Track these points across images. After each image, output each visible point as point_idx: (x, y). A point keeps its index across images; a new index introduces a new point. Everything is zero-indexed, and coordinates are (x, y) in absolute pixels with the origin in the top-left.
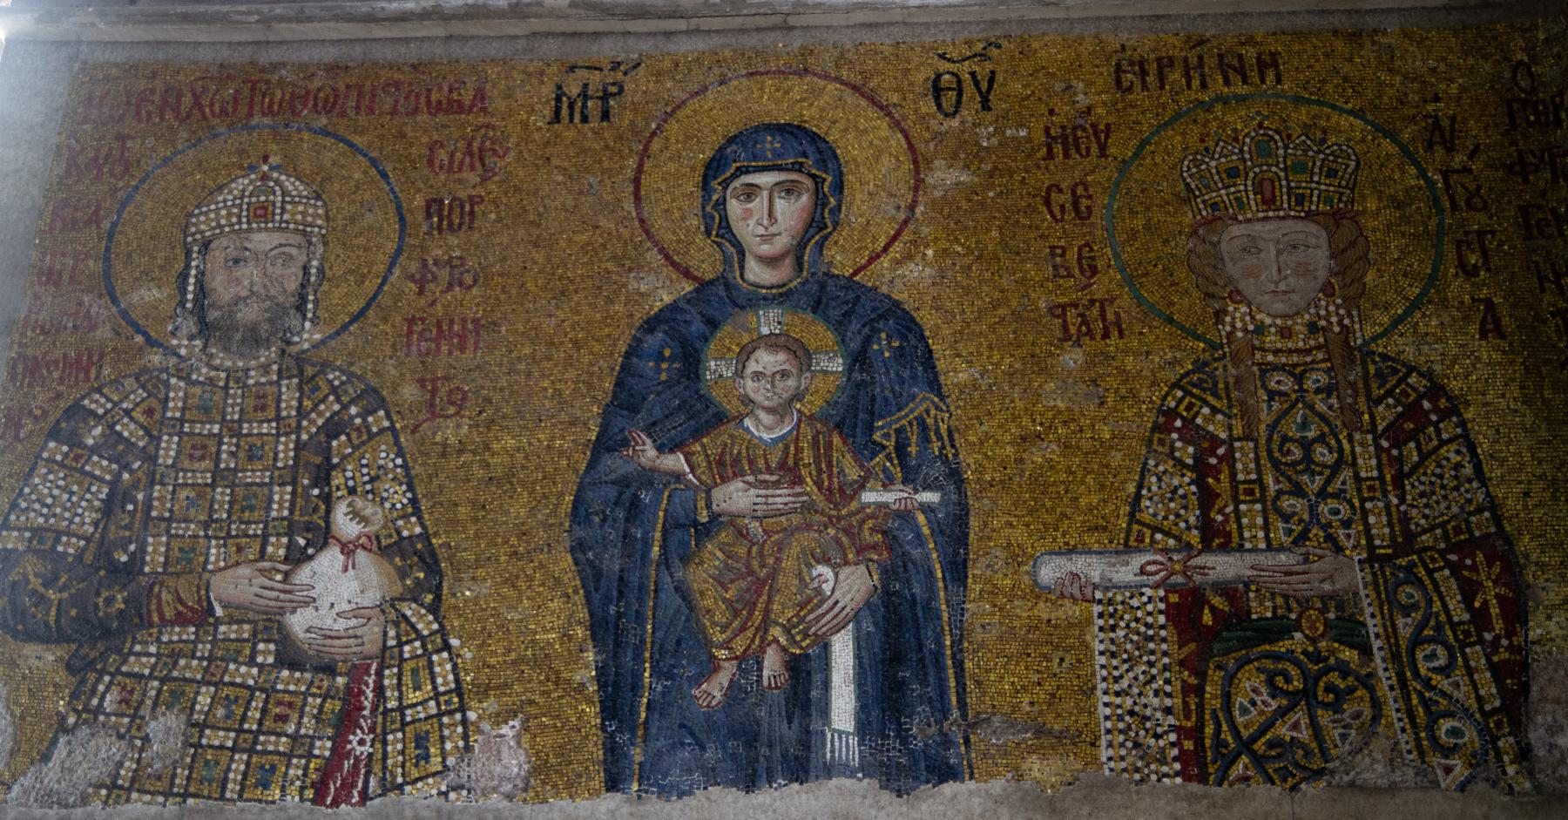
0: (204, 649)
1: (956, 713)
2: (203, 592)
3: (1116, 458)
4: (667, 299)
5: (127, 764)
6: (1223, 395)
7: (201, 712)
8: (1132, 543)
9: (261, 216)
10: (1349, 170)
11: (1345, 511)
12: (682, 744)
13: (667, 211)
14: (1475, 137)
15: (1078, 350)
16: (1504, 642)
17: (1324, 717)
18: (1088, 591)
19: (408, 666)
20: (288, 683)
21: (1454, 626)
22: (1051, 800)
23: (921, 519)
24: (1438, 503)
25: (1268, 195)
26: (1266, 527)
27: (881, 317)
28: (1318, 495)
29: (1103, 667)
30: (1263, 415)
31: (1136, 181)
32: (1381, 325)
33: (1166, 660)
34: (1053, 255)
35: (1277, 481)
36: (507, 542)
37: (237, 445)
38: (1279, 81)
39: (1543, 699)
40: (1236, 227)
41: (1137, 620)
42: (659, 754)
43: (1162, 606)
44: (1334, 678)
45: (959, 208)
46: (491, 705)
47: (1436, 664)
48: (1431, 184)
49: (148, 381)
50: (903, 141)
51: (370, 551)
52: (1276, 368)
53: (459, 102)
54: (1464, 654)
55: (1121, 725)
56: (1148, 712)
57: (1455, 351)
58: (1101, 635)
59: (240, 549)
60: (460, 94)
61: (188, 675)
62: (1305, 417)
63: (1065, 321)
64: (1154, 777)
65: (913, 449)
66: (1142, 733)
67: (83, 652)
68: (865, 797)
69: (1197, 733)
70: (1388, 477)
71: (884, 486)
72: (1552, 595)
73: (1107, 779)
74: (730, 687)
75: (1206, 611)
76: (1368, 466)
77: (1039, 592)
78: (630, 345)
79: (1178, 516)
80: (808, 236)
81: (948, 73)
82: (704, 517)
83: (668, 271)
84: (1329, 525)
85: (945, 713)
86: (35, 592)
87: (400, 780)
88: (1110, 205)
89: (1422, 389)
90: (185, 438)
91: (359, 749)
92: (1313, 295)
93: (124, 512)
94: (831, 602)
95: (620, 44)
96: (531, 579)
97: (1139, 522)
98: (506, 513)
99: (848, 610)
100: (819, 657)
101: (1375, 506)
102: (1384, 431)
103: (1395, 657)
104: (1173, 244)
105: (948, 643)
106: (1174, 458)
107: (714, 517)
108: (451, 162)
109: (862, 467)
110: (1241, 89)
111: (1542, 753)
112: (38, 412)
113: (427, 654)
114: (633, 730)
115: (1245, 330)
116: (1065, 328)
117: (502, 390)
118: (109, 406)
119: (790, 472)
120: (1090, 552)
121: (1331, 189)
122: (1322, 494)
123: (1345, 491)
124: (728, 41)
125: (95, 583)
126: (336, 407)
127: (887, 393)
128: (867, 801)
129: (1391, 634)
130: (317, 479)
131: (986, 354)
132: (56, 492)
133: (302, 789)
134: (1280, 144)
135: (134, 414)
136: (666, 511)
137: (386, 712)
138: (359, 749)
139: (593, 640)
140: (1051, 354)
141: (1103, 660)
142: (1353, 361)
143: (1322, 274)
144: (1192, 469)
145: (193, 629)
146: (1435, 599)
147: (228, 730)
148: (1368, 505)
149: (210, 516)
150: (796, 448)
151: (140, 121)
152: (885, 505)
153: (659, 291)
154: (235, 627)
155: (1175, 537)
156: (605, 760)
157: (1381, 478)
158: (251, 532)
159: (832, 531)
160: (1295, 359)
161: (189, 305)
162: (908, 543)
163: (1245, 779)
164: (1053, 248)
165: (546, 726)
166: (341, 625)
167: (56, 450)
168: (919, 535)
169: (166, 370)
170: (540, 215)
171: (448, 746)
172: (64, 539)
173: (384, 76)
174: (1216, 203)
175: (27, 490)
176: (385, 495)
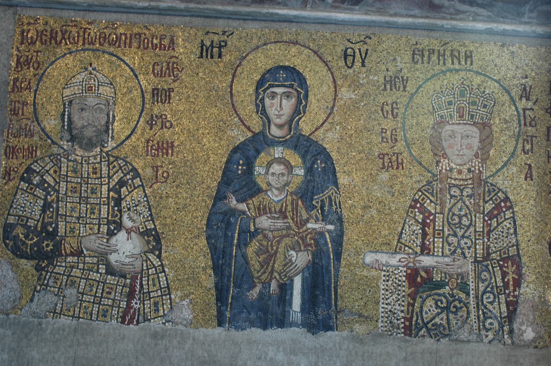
1: (333, 308)
4: (242, 139)
5: (58, 305)
6: (435, 195)
7: (81, 289)
10: (491, 106)
12: (243, 312)
13: (242, 101)
15: (387, 173)
16: (512, 294)
17: (451, 316)
18: (381, 267)
19: (151, 277)
21: (497, 287)
22: (361, 339)
23: (327, 236)
24: (500, 242)
26: (442, 248)
27: (319, 154)
28: (461, 237)
29: (383, 294)
30: (447, 205)
32: (492, 171)
33: (404, 294)
34: (382, 132)
35: (449, 230)
37: (87, 188)
38: (472, 64)
39: (520, 313)
41: (396, 278)
42: (235, 315)
43: (405, 274)
44: (457, 303)
45: (350, 109)
46: (179, 293)
47: (489, 300)
49: (53, 159)
50: (331, 78)
52: (455, 186)
53: (164, 45)
55: (386, 315)
56: (396, 311)
58: (384, 283)
59: (91, 229)
60: (164, 42)
62: (461, 206)
63: (384, 161)
64: (395, 334)
65: (326, 208)
66: (393, 318)
67: (41, 263)
68: (302, 334)
70: (485, 232)
71: (315, 221)
72: (530, 279)
73: (380, 334)
76: (479, 226)
77: (365, 266)
78: (228, 159)
79: (414, 241)
80: (294, 116)
81: (350, 48)
83: (242, 127)
84: (463, 248)
85: (330, 307)
86: (21, 240)
87: (149, 317)
88: (405, 113)
89: (502, 198)
90: (69, 184)
91: (135, 306)
92: (471, 157)
93: (49, 211)
94: (294, 265)
95: (226, 23)
96: (192, 248)
97: (401, 243)
98: (184, 222)
99: (300, 268)
100: (290, 284)
102: (487, 213)
103: (477, 297)
104: (425, 132)
106: (415, 219)
107: (256, 230)
108: (162, 72)
109: (308, 214)
111: (516, 331)
112: (16, 169)
115: (446, 170)
116: (383, 164)
117: (182, 173)
118: (41, 168)
119: (283, 215)
120: (383, 252)
121: (484, 113)
122: (463, 237)
123: (470, 236)
124: (267, 25)
125: (42, 238)
126: (122, 175)
129: (477, 289)
130: (117, 203)
132: (25, 202)
133: (117, 318)
134: (468, 92)
135: (49, 172)
136: (239, 226)
137: (144, 293)
138: (135, 306)
140: (377, 174)
141: (383, 292)
142: (481, 185)
143: (475, 148)
147: (91, 296)
148: (477, 241)
149: (80, 215)
150: (286, 204)
151: (42, 44)
154: (91, 258)
155: (412, 249)
156: (217, 315)
157: (483, 231)
158: (94, 223)
160: (461, 183)
161: (66, 127)
162: (323, 244)
163: (423, 336)
164: (382, 129)
165: (197, 302)
166: (127, 260)
168: (326, 241)
169: (59, 154)
170: (195, 99)
171: (165, 306)
172: (30, 220)
173: (136, 30)
175: (15, 201)
176: (141, 212)
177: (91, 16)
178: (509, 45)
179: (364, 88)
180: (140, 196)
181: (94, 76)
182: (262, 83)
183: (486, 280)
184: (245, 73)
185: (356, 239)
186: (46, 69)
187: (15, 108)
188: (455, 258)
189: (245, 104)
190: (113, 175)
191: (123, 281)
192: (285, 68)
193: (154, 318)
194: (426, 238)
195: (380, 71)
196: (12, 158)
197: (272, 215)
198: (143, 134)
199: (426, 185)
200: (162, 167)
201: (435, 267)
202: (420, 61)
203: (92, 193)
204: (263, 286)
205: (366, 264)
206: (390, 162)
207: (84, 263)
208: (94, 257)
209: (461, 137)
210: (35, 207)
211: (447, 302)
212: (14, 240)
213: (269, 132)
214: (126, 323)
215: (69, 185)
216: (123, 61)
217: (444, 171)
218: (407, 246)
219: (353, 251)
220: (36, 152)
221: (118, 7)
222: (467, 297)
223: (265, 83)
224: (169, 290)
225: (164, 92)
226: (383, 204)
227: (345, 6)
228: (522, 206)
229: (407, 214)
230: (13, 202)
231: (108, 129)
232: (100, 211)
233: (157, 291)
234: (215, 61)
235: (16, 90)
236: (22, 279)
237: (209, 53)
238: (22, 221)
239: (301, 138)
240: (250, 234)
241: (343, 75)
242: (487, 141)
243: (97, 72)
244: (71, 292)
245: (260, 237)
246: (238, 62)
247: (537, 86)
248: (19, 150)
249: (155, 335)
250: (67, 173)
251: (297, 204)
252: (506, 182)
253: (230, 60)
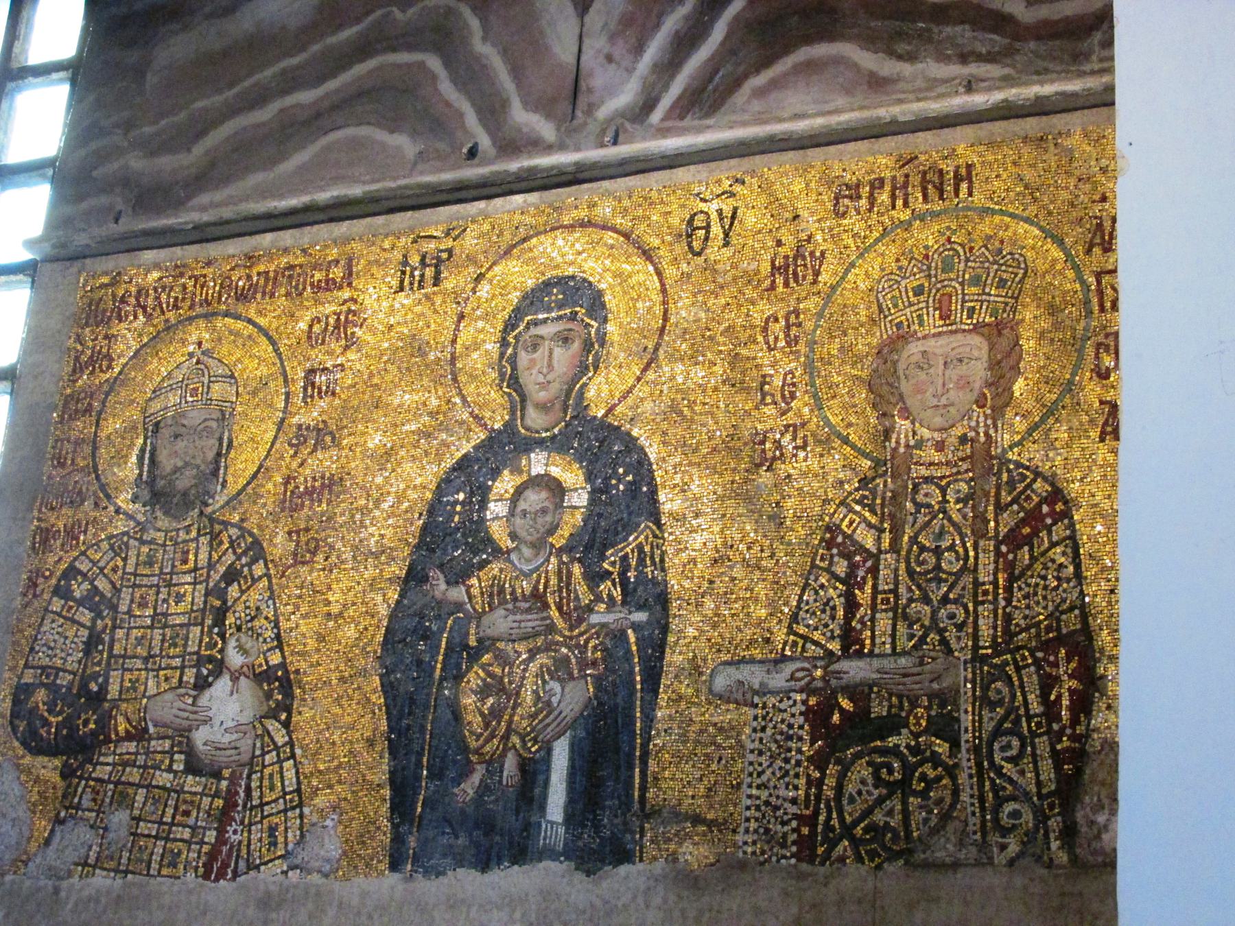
0: (141, 760)
1: (636, 806)
5: (94, 847)
10: (1017, 279)
16: (1068, 731)
19: (267, 771)
22: (696, 878)
23: (632, 637)
25: (945, 309)
26: (893, 636)
29: (751, 763)
35: (910, 590)
37: (169, 594)
38: (970, 194)
40: (913, 345)
42: (426, 841)
47: (1008, 754)
48: (1086, 286)
50: (658, 284)
51: (248, 677)
52: (927, 480)
55: (758, 814)
56: (779, 802)
62: (943, 526)
64: (774, 859)
65: (631, 575)
66: (773, 820)
68: (563, 876)
69: (812, 821)
81: (702, 212)
82: (472, 642)
84: (945, 629)
86: (42, 716)
87: (258, 861)
91: (233, 837)
92: (967, 407)
94: (556, 713)
97: (796, 634)
98: (340, 644)
100: (543, 759)
103: (976, 750)
110: (937, 206)
111: (1084, 829)
112: (47, 573)
113: (280, 761)
128: (565, 880)
132: (57, 637)
138: (233, 837)
141: (751, 757)
145: (135, 744)
159: (564, 650)
161: (145, 477)
163: (842, 859)
164: (764, 376)
166: (227, 739)
167: (57, 604)
168: (629, 651)
171: (290, 835)
172: (61, 674)
177: (213, 250)
178: (1060, 134)
187: (60, 453)
188: (924, 656)
193: (266, 863)
194: (854, 616)
204: (487, 770)
209: (946, 363)
214: (213, 877)
217: (902, 450)
221: (246, 219)
222: (954, 749)
224: (300, 798)
226: (757, 548)
227: (687, 122)
228: (1096, 505)
230: (36, 639)
231: (218, 469)
232: (187, 639)
233: (275, 801)
240: (468, 653)
244: (120, 818)
245: (486, 658)
249: (267, 902)
251: (570, 574)
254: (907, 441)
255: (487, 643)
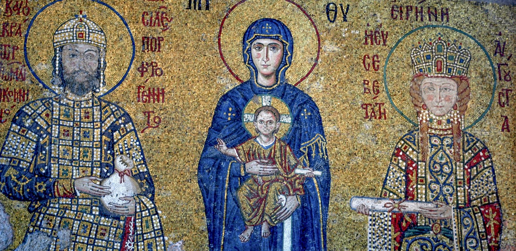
2: (72, 187)
3: (380, 165)
4: (231, 88)
5: (52, 246)
7: (75, 230)
8: (383, 196)
9: (80, 37)
10: (468, 60)
11: (451, 190)
13: (230, 51)
14: (511, 51)
15: (370, 122)
16: (494, 239)
18: (367, 211)
19: (144, 219)
20: (104, 222)
21: (479, 232)
23: (315, 181)
24: (480, 189)
26: (426, 194)
27: (305, 103)
29: (370, 238)
30: (429, 153)
31: (395, 56)
33: (390, 237)
34: (364, 83)
35: (431, 178)
36: (176, 177)
37: (80, 131)
38: (448, 21)
41: (382, 223)
43: (390, 219)
45: (333, 61)
46: (173, 235)
47: (472, 245)
49: (45, 102)
50: (315, 31)
52: (435, 135)
54: (481, 242)
57: (493, 135)
58: (370, 227)
59: (83, 172)
61: (70, 216)
62: (442, 155)
63: (367, 111)
65: (313, 155)
67: (33, 205)
70: (466, 179)
71: (303, 167)
72: (510, 225)
74: (251, 235)
75: (404, 221)
76: (460, 174)
77: (352, 210)
78: (218, 106)
79: (398, 187)
80: (280, 67)
81: (332, 3)
83: (231, 76)
84: (446, 195)
86: (14, 182)
90: (61, 127)
92: (450, 109)
94: (284, 208)
96: (185, 192)
97: (385, 189)
98: (176, 166)
99: (290, 212)
100: (280, 227)
101: (460, 189)
102: (467, 162)
103: (460, 242)
104: (405, 84)
105: (322, 226)
106: (399, 166)
107: (246, 174)
108: (151, 22)
109: (296, 160)
112: (7, 112)
114: (219, 247)
115: (426, 120)
116: (367, 114)
117: (173, 119)
120: (368, 198)
123: (452, 183)
125: (35, 180)
126: (114, 120)
127: (306, 133)
130: (109, 147)
131: (340, 121)
132: (17, 144)
134: (445, 47)
135: (41, 115)
136: (230, 170)
137: (137, 235)
139: (206, 215)
140: (361, 123)
141: (370, 236)
143: (453, 100)
144: (404, 171)
145: (70, 200)
146: (475, 223)
147: (85, 237)
148: (459, 189)
149: (72, 158)
150: (274, 150)
152: (303, 175)
153: (228, 84)
154: (84, 200)
155: (396, 195)
157: (464, 179)
158: (87, 165)
159: (285, 182)
160: (441, 133)
161: (57, 72)
162: (311, 189)
164: (365, 81)
165: (191, 244)
166: (121, 202)
167: (15, 127)
168: (314, 187)
169: (51, 98)
170: (184, 48)
171: (159, 248)
172: (22, 162)
174: (421, 69)
175: (7, 143)
176: (133, 155)
178: (483, 3)
179: (346, 41)
180: (132, 140)
181: (84, 23)
182: (249, 35)
183: (468, 225)
184: (232, 24)
185: (343, 185)
186: (36, 15)
187: (5, 52)
188: (437, 205)
189: (233, 53)
190: (105, 120)
191: (117, 223)
192: (271, 21)
195: (361, 25)
196: (4, 101)
197: (262, 160)
198: (134, 80)
199: (408, 134)
200: (153, 112)
201: (419, 213)
202: (399, 17)
203: (85, 137)
204: (254, 229)
205: (353, 209)
206: (373, 112)
207: (78, 205)
208: (87, 199)
210: (27, 149)
211: (432, 247)
212: (6, 181)
213: (257, 81)
215: (62, 129)
216: (113, 10)
217: (424, 121)
218: (392, 192)
219: (339, 196)
220: (28, 95)
222: (451, 241)
223: (251, 34)
224: (162, 232)
225: (154, 41)
226: (367, 152)
228: (500, 156)
229: (391, 161)
230: (5, 144)
231: (100, 76)
232: (93, 154)
234: (202, 13)
235: (6, 34)
236: (15, 220)
237: (197, 4)
238: (14, 162)
239: (287, 87)
240: (240, 179)
241: (326, 29)
242: (465, 94)
243: (87, 19)
244: (63, 234)
245: (250, 181)
246: (225, 14)
247: (511, 43)
248: (11, 93)
250: (59, 117)
252: (484, 133)
253: (217, 11)
254: (426, 118)
255: (250, 175)
